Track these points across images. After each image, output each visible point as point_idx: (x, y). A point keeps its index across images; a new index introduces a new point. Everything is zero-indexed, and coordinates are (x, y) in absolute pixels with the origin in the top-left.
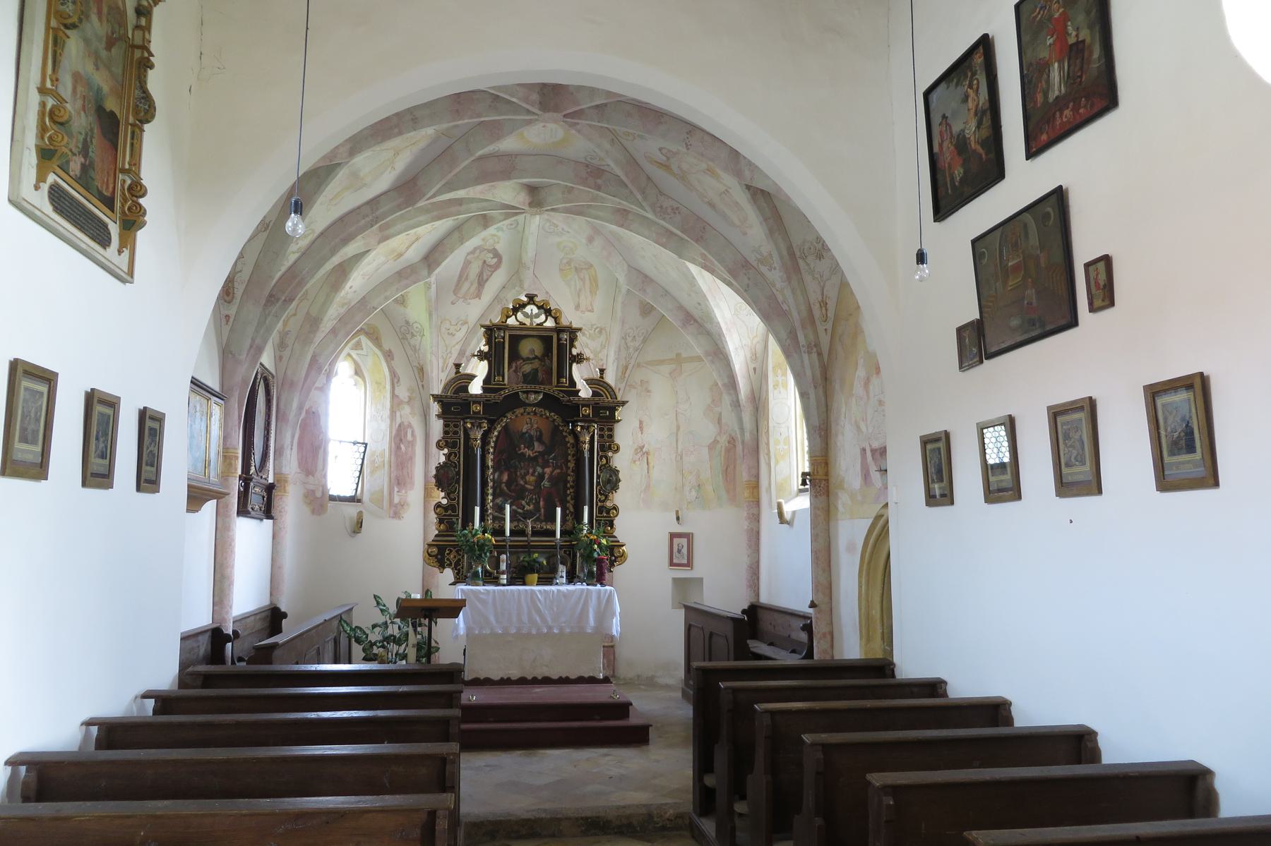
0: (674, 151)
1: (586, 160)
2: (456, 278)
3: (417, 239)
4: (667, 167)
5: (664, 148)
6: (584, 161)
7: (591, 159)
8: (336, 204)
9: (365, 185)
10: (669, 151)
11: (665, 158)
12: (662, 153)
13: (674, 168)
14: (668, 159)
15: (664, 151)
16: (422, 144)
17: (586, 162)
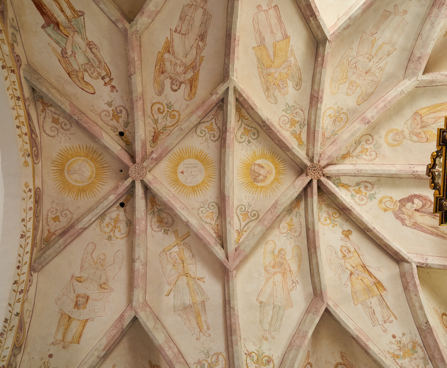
0: (170, 81)
1: (217, 140)
2: (432, 237)
3: (364, 267)
4: (192, 83)
5: (171, 88)
6: (218, 143)
7: (214, 136)
8: (208, 329)
9: (203, 302)
10: (172, 84)
11: (183, 86)
12: (179, 89)
13: (190, 75)
14: (181, 83)
15: (175, 87)
16: (187, 254)
17: (220, 140)
